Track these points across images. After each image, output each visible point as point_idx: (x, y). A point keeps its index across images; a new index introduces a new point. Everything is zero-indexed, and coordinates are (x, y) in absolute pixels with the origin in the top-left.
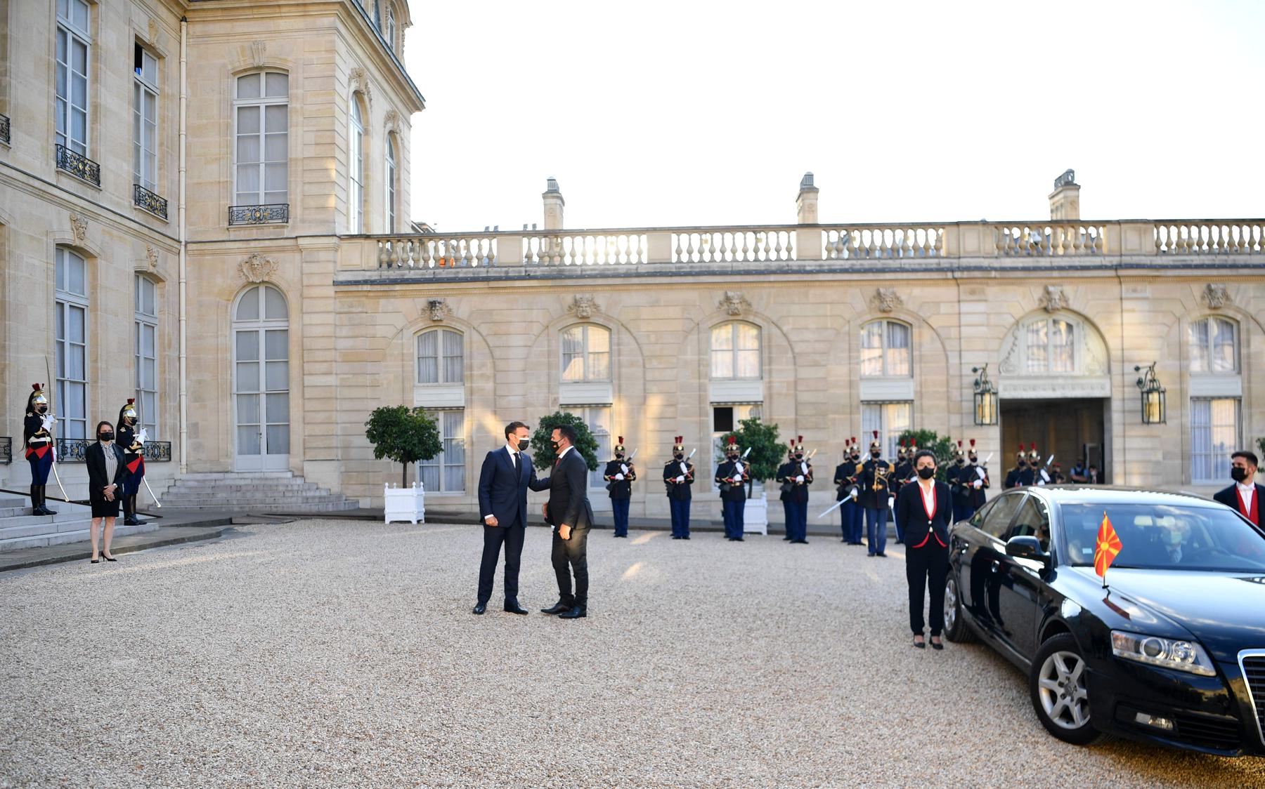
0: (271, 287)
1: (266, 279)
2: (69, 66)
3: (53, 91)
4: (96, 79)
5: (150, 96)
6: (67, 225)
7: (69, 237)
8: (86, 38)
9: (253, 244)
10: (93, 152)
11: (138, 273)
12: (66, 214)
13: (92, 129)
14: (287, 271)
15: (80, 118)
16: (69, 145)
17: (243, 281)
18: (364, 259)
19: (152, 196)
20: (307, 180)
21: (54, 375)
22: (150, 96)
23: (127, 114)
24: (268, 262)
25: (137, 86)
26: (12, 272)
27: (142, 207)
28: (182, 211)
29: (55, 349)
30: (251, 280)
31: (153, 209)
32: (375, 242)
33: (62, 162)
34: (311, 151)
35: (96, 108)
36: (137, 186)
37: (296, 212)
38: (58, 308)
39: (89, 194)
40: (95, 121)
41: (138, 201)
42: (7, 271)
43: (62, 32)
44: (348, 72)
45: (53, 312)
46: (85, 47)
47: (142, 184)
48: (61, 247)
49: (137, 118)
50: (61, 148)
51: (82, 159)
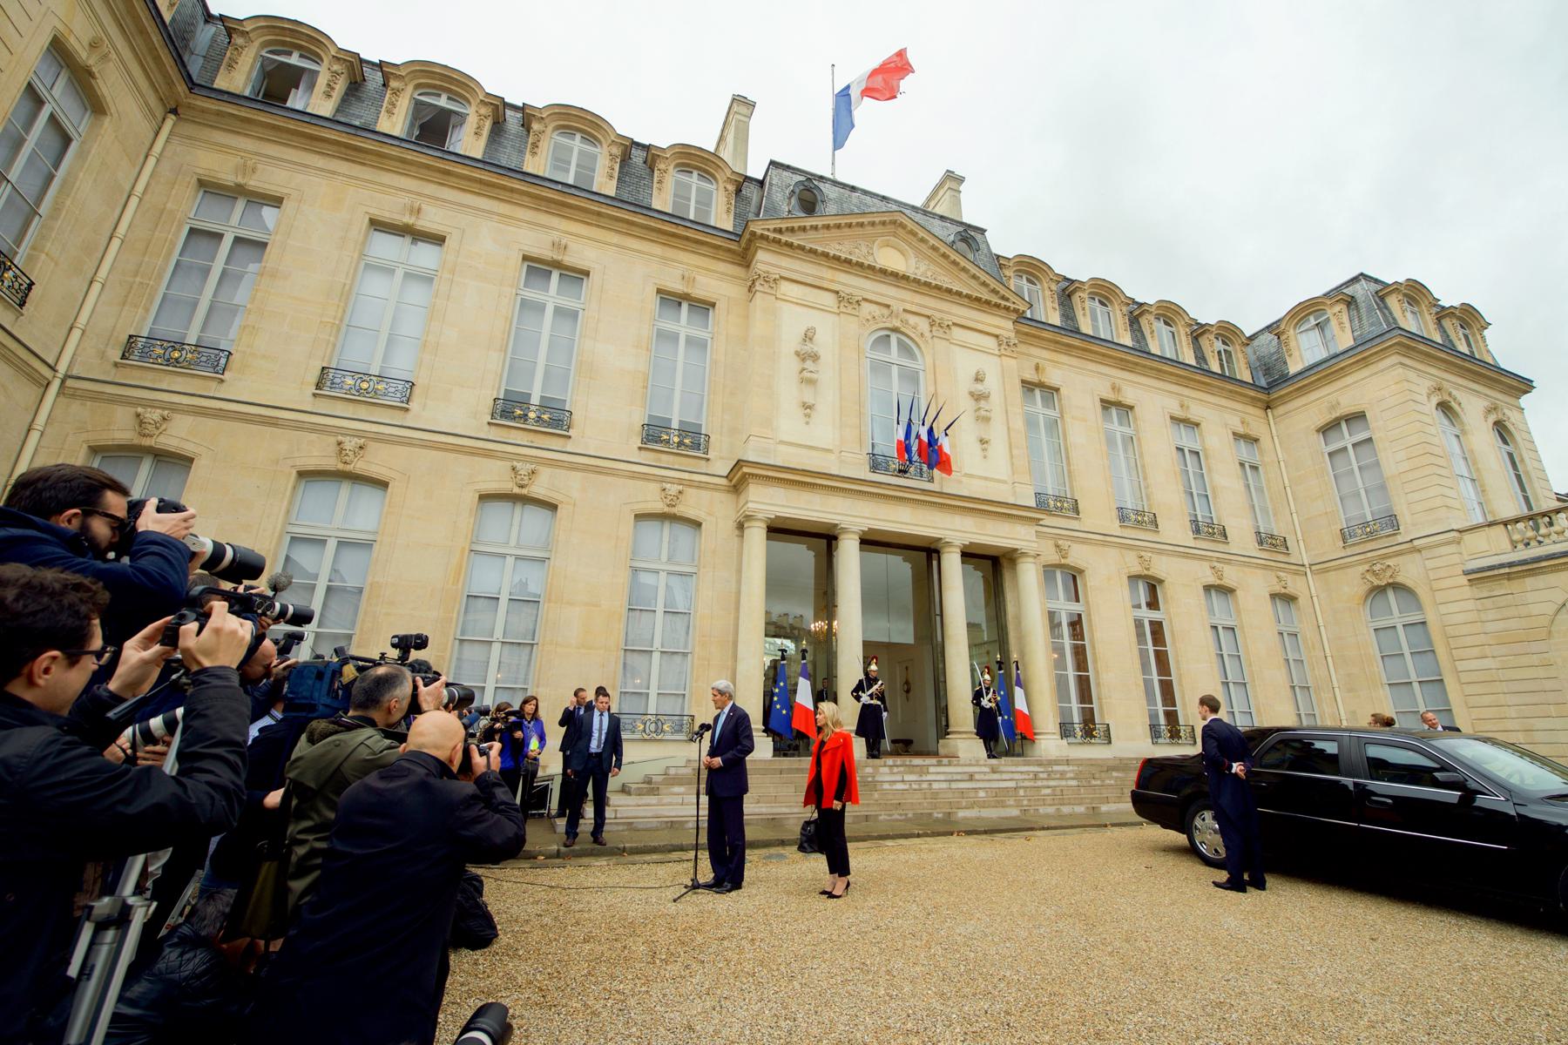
0: (1397, 587)
1: (1391, 581)
2: (1190, 468)
3: (1181, 488)
4: (1209, 470)
5: (1255, 468)
6: (1209, 572)
7: (1212, 580)
8: (1197, 447)
9: (1369, 555)
10: (1219, 519)
11: (1273, 596)
12: (1206, 565)
13: (1214, 504)
14: (1409, 571)
15: (1205, 500)
16: (1200, 519)
17: (1369, 586)
18: (1495, 547)
19: (1272, 537)
20: (1406, 491)
21: (1218, 679)
22: (1255, 468)
23: (1239, 485)
24: (1389, 566)
25: (1242, 465)
27: (1265, 546)
28: (1301, 543)
29: (1215, 661)
30: (1375, 584)
31: (1275, 546)
32: (1502, 526)
33: (1197, 531)
34: (1406, 466)
35: (1214, 489)
36: (1258, 533)
37: (1405, 519)
38: (1214, 630)
39: (1221, 547)
40: (1215, 498)
41: (1261, 543)
43: (1180, 450)
44: (1425, 391)
45: (1210, 634)
46: (1198, 453)
47: (1262, 530)
48: (1208, 588)
49: (1248, 486)
50: (1195, 522)
51: (1210, 525)
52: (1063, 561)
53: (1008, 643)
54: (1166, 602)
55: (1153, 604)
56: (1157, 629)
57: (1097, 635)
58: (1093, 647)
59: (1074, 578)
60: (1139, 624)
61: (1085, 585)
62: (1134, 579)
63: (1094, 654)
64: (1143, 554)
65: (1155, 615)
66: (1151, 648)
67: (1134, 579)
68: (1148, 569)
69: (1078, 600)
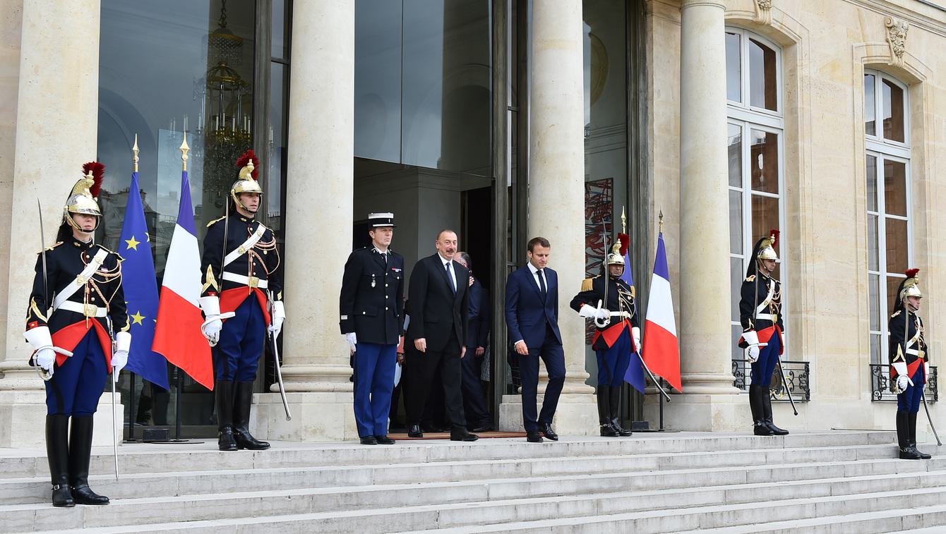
26: (931, 143)
42: (926, 142)
52: (762, 16)
53: (646, 185)
54: (917, 125)
55: (894, 129)
56: (896, 172)
57: (808, 182)
58: (795, 206)
59: (770, 57)
60: (872, 162)
61: (792, 73)
62: (873, 70)
63: (795, 220)
64: (895, 21)
65: (895, 151)
66: (882, 215)
67: (873, 70)
68: (899, 54)
69: (771, 103)
